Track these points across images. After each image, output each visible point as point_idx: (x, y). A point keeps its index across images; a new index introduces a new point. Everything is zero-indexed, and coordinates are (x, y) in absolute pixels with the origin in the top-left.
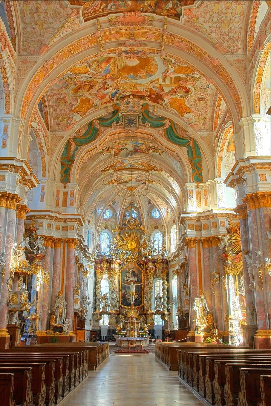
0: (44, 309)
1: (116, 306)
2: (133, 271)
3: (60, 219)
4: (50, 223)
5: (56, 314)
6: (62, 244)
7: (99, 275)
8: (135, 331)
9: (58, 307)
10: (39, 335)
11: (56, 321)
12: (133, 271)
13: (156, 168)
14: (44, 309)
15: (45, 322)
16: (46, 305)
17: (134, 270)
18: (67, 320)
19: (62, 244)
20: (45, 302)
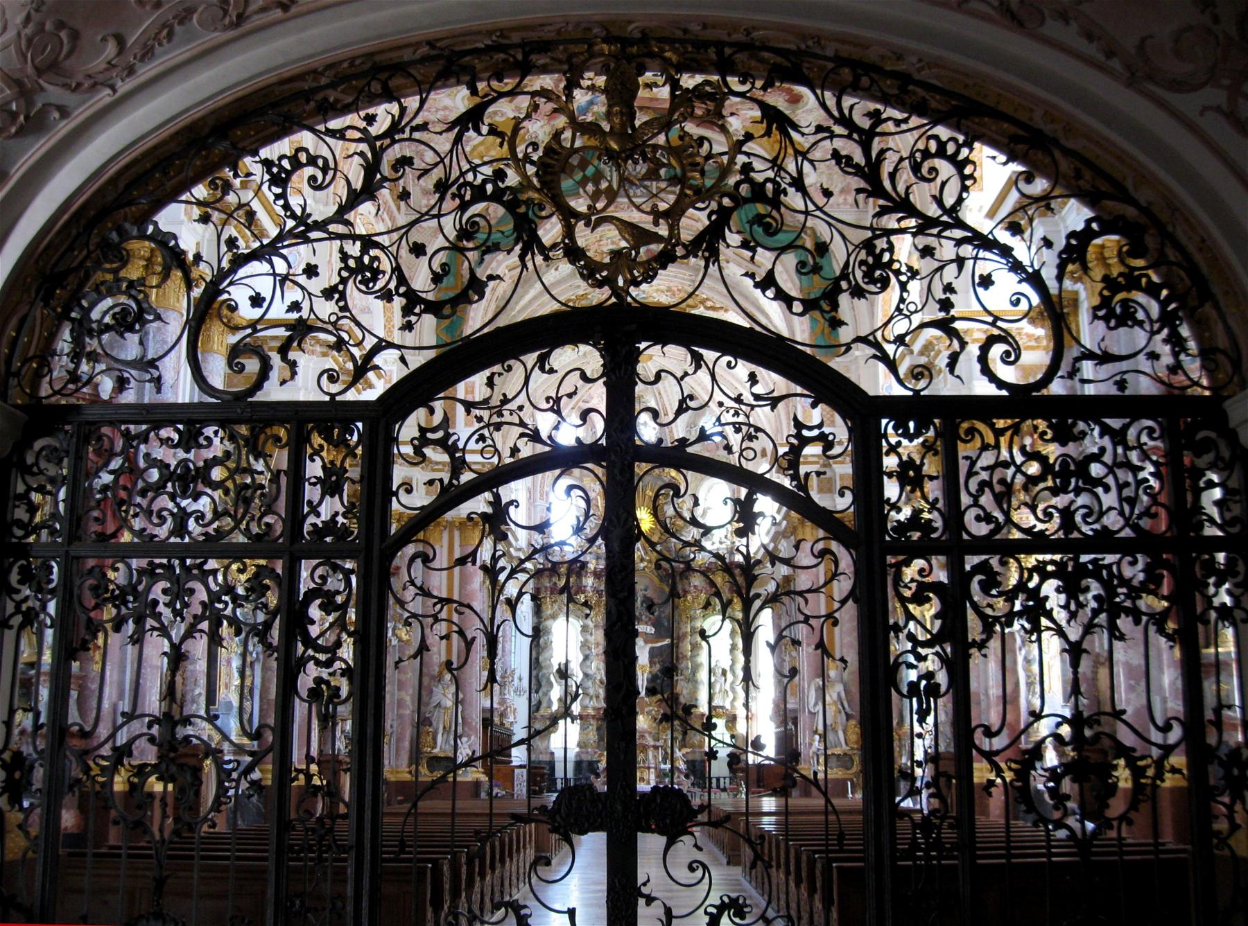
0: (401, 711)
1: (597, 697)
2: (645, 596)
3: (437, 463)
4: (409, 474)
5: (434, 723)
6: (446, 535)
7: (548, 610)
8: (649, 768)
9: (439, 705)
10: (393, 779)
11: (435, 739)
12: (645, 596)
13: (709, 304)
14: (401, 711)
15: (407, 744)
16: (408, 699)
17: (650, 594)
18: (464, 739)
19: (446, 535)
20: (403, 694)
